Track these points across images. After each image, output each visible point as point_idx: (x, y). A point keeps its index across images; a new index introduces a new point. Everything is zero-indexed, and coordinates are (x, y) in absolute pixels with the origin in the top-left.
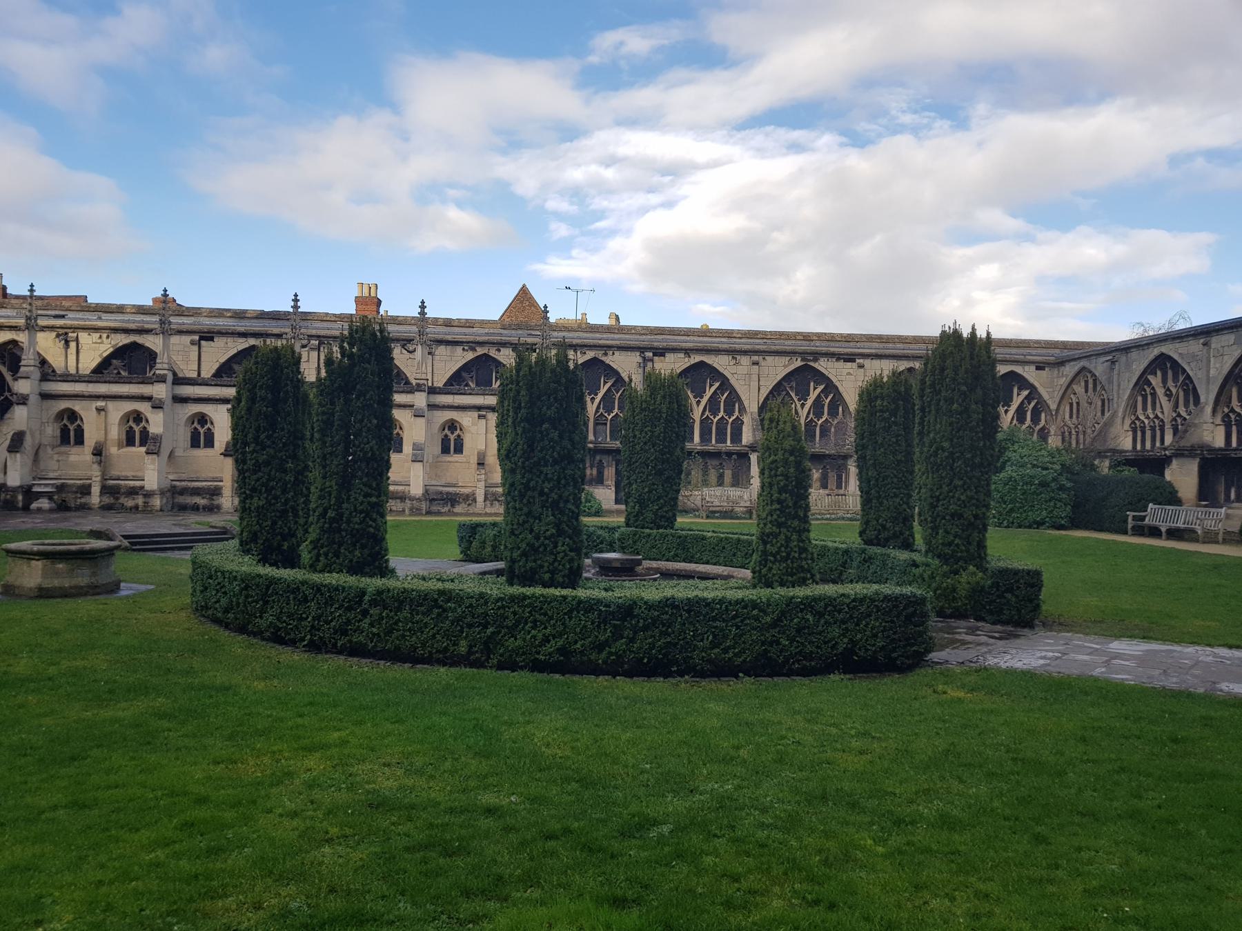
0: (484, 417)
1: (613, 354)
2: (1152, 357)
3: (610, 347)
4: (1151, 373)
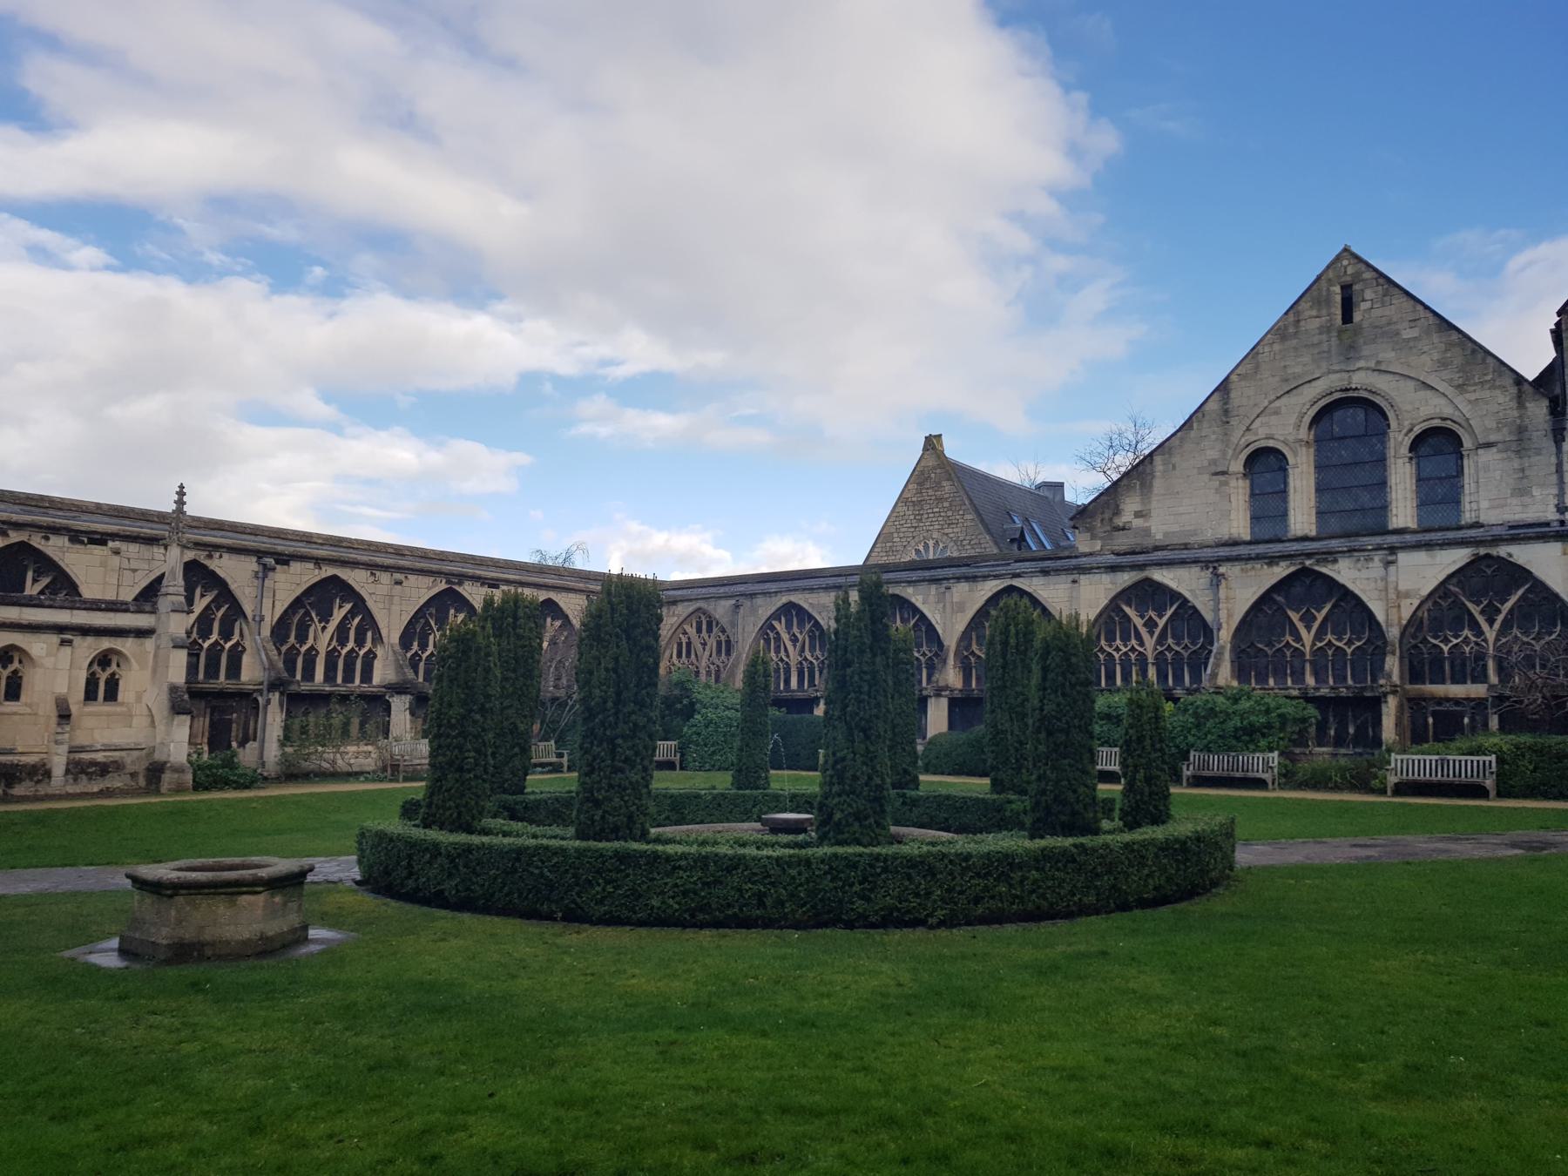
0: (70, 642)
1: (221, 557)
2: (779, 604)
3: (217, 547)
4: (775, 619)
